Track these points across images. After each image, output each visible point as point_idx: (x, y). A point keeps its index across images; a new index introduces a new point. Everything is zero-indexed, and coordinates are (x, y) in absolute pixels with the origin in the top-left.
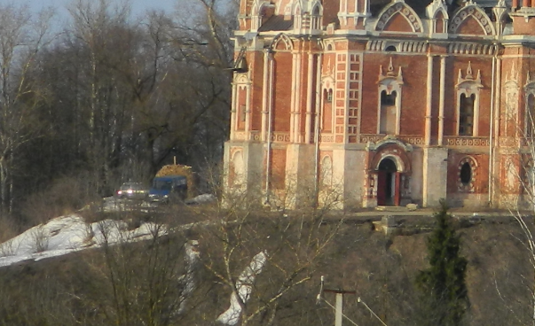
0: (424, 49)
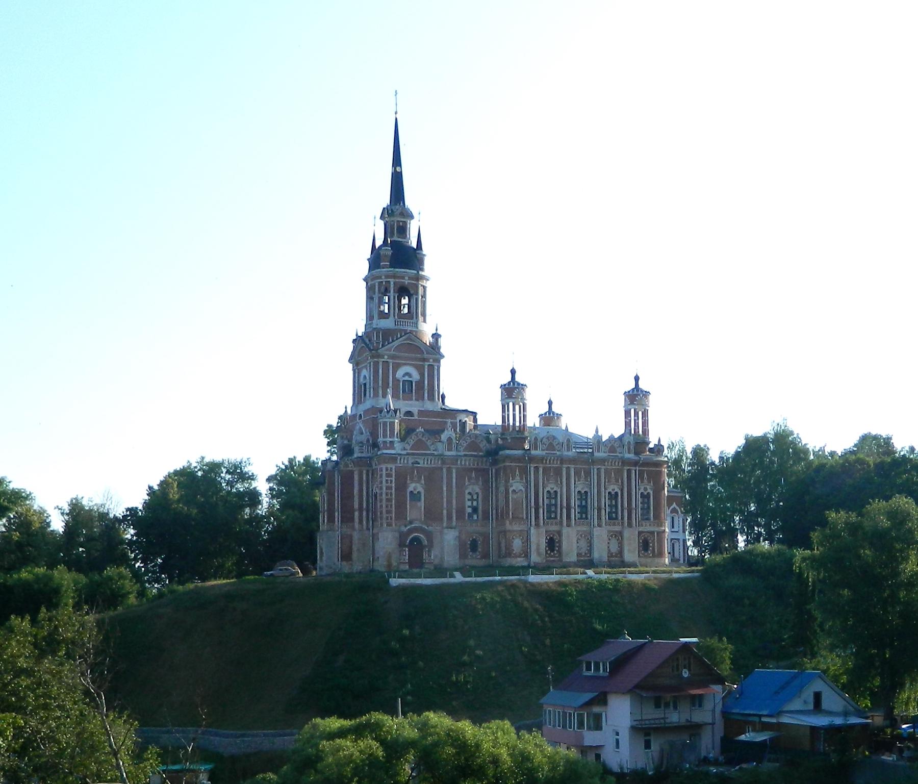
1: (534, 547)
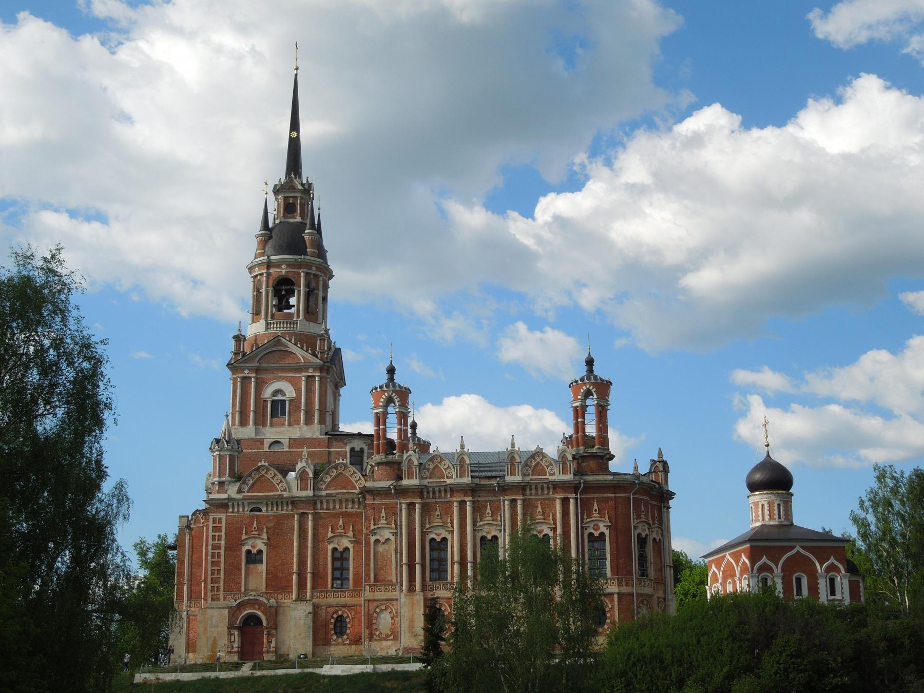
0: (290, 508)
1: (405, 625)
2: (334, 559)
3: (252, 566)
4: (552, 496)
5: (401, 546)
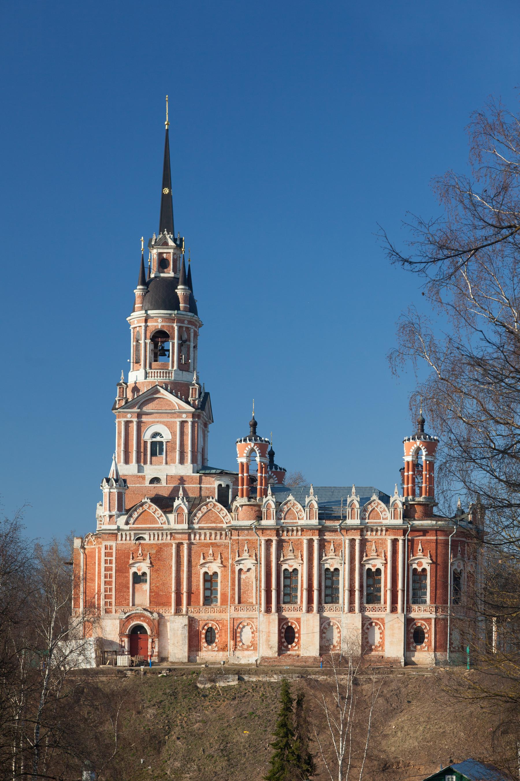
0: (169, 537)
2: (205, 581)
3: (137, 586)
4: (383, 537)
5: (260, 574)
